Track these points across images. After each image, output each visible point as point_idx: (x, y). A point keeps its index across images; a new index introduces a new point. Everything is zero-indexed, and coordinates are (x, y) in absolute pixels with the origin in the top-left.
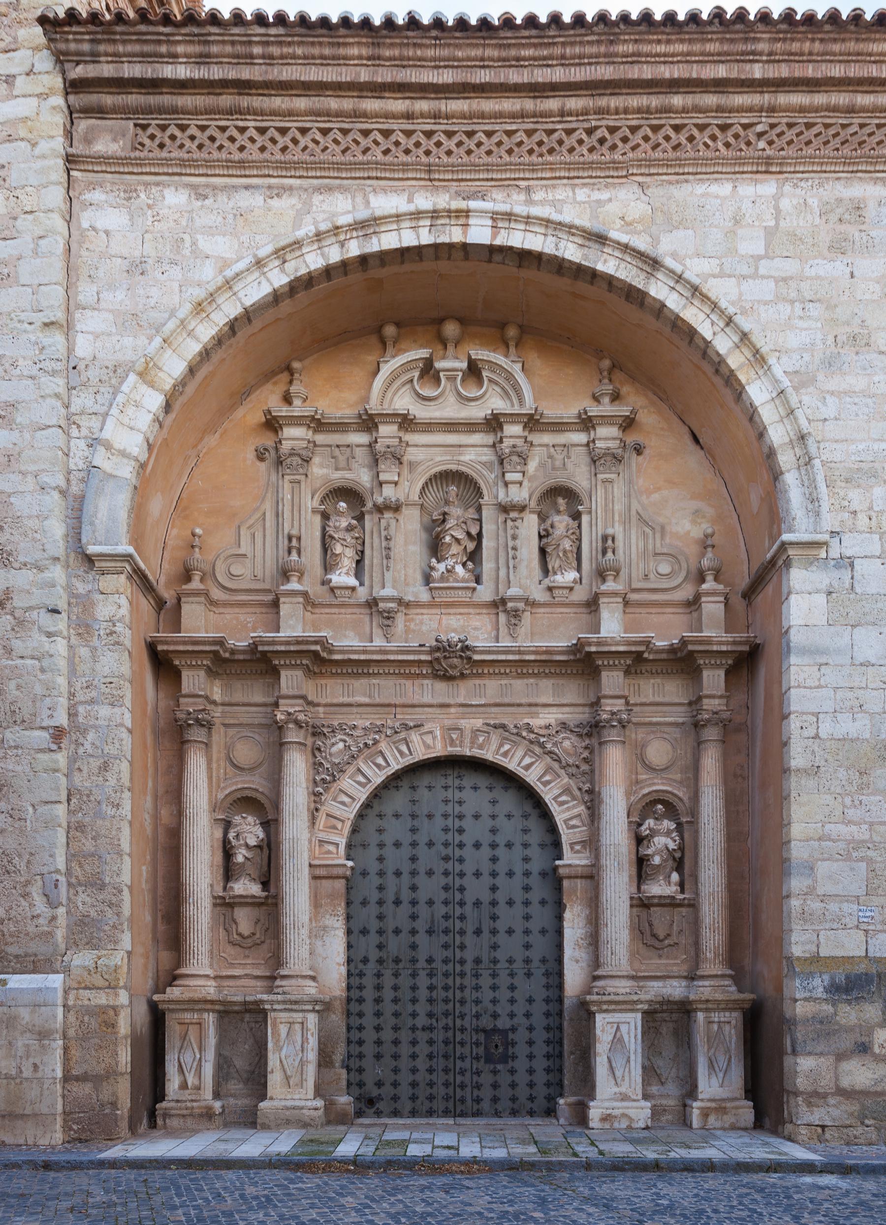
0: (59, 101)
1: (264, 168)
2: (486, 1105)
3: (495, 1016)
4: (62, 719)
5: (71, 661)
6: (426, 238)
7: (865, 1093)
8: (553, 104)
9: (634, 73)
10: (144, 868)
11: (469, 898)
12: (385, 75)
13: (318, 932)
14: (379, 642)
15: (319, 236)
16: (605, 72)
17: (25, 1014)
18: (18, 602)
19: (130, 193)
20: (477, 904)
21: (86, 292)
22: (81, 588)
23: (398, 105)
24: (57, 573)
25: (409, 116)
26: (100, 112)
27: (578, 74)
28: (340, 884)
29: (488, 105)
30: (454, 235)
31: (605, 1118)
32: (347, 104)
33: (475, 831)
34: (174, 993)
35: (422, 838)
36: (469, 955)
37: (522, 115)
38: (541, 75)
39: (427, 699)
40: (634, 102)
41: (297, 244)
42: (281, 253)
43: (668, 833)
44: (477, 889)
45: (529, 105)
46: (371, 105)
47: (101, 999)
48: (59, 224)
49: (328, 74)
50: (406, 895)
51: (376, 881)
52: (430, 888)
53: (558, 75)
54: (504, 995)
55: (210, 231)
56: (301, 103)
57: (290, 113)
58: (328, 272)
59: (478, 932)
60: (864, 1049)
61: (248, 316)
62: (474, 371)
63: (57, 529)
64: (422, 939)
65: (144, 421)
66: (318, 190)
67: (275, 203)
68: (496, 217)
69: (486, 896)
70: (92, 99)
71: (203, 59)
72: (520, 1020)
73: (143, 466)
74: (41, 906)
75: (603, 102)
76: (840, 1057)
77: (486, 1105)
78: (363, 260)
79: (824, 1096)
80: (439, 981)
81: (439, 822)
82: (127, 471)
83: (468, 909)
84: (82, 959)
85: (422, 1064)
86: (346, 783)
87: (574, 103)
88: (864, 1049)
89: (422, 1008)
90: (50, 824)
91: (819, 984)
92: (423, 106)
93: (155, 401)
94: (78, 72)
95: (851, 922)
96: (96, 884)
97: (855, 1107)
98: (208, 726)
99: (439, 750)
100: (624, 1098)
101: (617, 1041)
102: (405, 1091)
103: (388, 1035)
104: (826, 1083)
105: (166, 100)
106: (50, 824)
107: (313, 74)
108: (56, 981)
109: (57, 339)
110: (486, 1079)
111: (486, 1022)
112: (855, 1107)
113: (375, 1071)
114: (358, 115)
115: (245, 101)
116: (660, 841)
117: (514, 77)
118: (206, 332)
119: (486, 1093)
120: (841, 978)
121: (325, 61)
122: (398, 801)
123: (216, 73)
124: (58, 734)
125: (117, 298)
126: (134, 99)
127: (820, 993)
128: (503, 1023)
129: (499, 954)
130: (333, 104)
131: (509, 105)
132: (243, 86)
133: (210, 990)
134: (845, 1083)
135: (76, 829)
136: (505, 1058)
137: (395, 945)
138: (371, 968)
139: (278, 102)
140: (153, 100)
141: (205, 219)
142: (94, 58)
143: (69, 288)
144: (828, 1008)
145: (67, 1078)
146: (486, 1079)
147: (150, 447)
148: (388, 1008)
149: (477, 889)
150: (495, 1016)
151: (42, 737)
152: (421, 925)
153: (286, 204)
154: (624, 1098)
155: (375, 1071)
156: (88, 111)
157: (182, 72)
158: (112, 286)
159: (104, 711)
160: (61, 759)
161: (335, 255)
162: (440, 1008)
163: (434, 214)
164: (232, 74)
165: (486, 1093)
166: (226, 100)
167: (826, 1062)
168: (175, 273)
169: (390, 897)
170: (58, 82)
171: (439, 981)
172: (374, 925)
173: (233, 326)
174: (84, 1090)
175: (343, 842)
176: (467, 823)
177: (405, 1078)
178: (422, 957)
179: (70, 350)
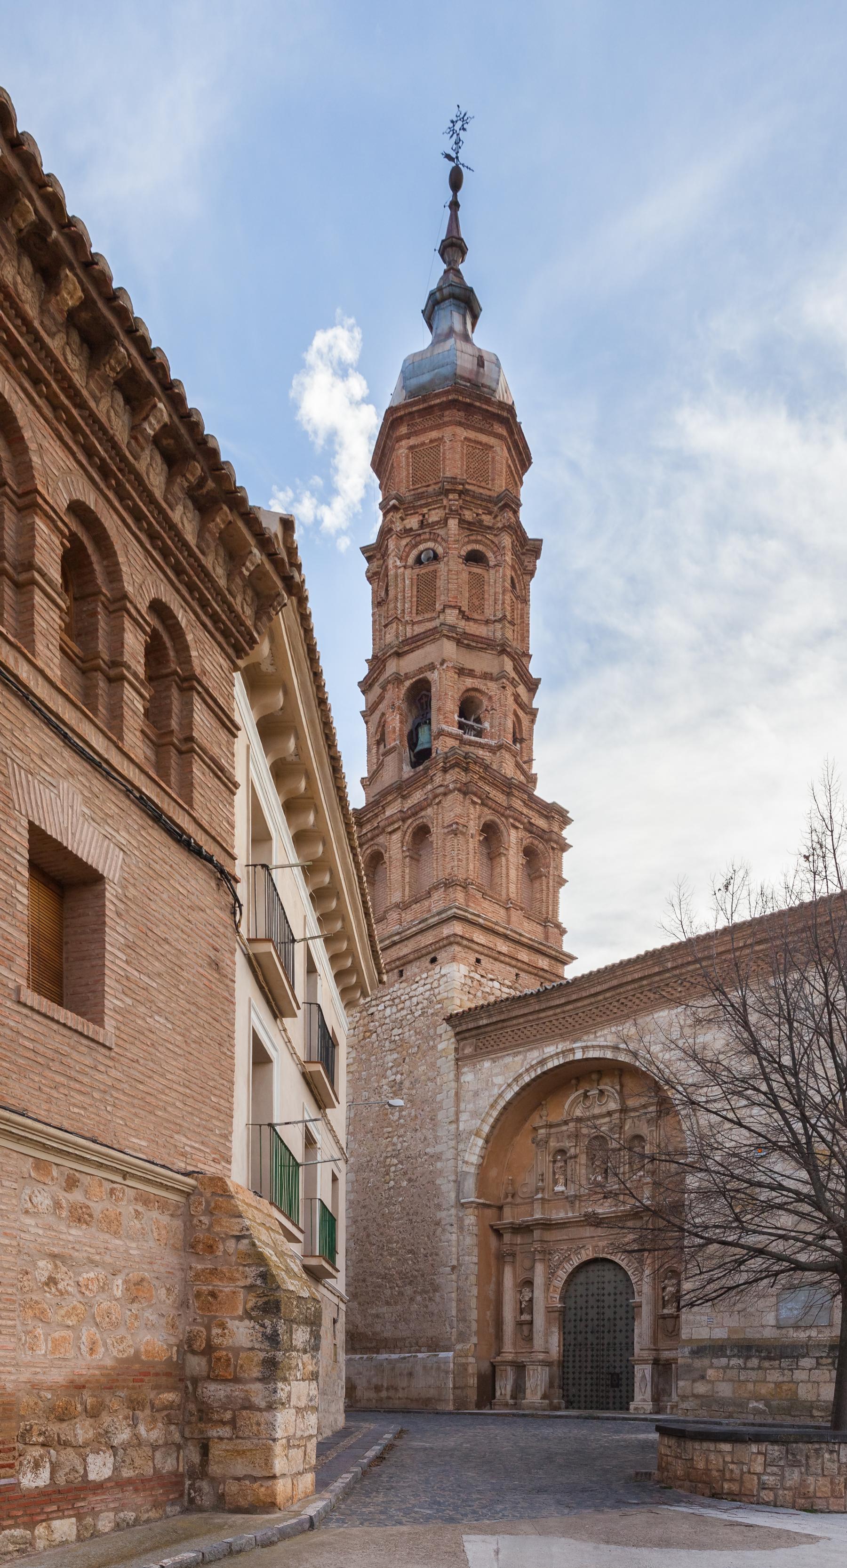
0: (453, 1040)
1: (510, 1047)
2: (611, 1405)
3: (615, 1367)
4: (455, 1263)
5: (458, 1241)
6: (562, 1061)
7: (702, 1396)
8: (600, 997)
9: (625, 980)
10: (488, 1313)
11: (606, 1317)
12: (544, 1006)
13: (547, 1334)
14: (570, 1214)
15: (527, 1070)
16: (615, 982)
17: (442, 1366)
18: (443, 1223)
19: (474, 1065)
20: (609, 1319)
21: (462, 1106)
22: (461, 1214)
23: (551, 1012)
24: (453, 1211)
25: (555, 1015)
26: (465, 1039)
27: (605, 986)
28: (557, 1314)
29: (579, 1004)
30: (571, 1058)
31: (636, 1409)
32: (535, 1017)
33: (609, 1288)
34: (499, 1359)
35: (590, 1293)
36: (606, 1342)
37: (592, 1004)
38: (593, 991)
39: (588, 1235)
40: (629, 988)
41: (521, 1075)
42: (516, 1080)
43: (673, 1285)
44: (609, 1313)
45: (593, 1000)
46: (542, 1015)
47: (463, 1360)
48: (453, 1084)
49: (526, 1011)
50: (584, 1317)
51: (573, 1311)
52: (592, 1313)
53: (599, 988)
54: (618, 1358)
55: (497, 1075)
56: (521, 1020)
57: (519, 1024)
58: (533, 1080)
59: (609, 1332)
60: (703, 1377)
61: (509, 1103)
62: (602, 1092)
63: (453, 1195)
64: (589, 1336)
65: (477, 1150)
66: (529, 1050)
67: (516, 1059)
68: (584, 1049)
69: (612, 1317)
70: (462, 1036)
71: (490, 1016)
72: (624, 1369)
73: (481, 1165)
74: (448, 1329)
75: (618, 991)
76: (694, 1381)
77: (611, 1405)
78: (544, 1073)
79: (688, 1397)
80: (595, 1353)
81: (596, 1285)
82: (472, 1170)
83: (606, 1322)
84: (459, 1347)
85: (588, 1388)
86: (560, 1273)
87: (608, 995)
88: (703, 1377)
89: (589, 1364)
90: (450, 1300)
91: (687, 1350)
92: (559, 1010)
93: (480, 1142)
94: (458, 1029)
95: (704, 1324)
96: (464, 1320)
97: (698, 1402)
98: (513, 1255)
99: (591, 1255)
100: (644, 1400)
101: (644, 1376)
102: (583, 1399)
103: (577, 1375)
104: (688, 1392)
105: (483, 1030)
106: (450, 1300)
107: (522, 1011)
108: (451, 1354)
109: (454, 1126)
110: (611, 1394)
111: (611, 1370)
112: (698, 1402)
113: (573, 1390)
114: (539, 1019)
115: (505, 1024)
116: (669, 1289)
117: (584, 994)
118: (495, 1114)
119: (611, 1400)
120: (695, 1348)
121: (524, 1006)
122: (581, 1278)
123: (494, 1019)
124: (453, 1268)
125: (470, 1107)
126: (474, 1033)
127: (687, 1354)
128: (618, 1370)
129: (617, 1341)
130: (531, 1018)
131: (586, 1002)
132: (503, 1021)
133: (510, 1357)
134: (695, 1392)
135: (459, 1301)
136: (618, 1386)
137: (580, 1338)
138: (571, 1348)
139: (515, 1022)
140: (479, 1031)
141: (496, 1070)
142: (460, 1024)
143: (457, 1106)
144: (690, 1361)
145: (454, 1388)
146: (611, 1394)
147: (483, 1157)
148: (577, 1364)
149: (609, 1313)
150: (615, 1367)
151: (449, 1269)
152: (589, 1329)
153: (519, 1058)
154: (644, 1400)
155: (573, 1390)
156: (462, 1039)
157: (485, 1022)
158: (469, 1103)
159: (467, 1258)
160: (454, 1277)
161: (533, 1075)
162: (595, 1364)
163: (563, 1052)
164: (499, 1019)
165: (611, 1400)
166: (500, 1026)
167: (689, 1383)
168: (487, 1093)
169: (578, 1318)
170: (452, 1033)
171: (595, 1353)
172: (573, 1330)
173: (505, 1108)
174: (458, 1392)
175: (558, 1297)
176: (606, 1285)
177: (583, 1394)
178: (589, 1342)
179: (458, 1128)
